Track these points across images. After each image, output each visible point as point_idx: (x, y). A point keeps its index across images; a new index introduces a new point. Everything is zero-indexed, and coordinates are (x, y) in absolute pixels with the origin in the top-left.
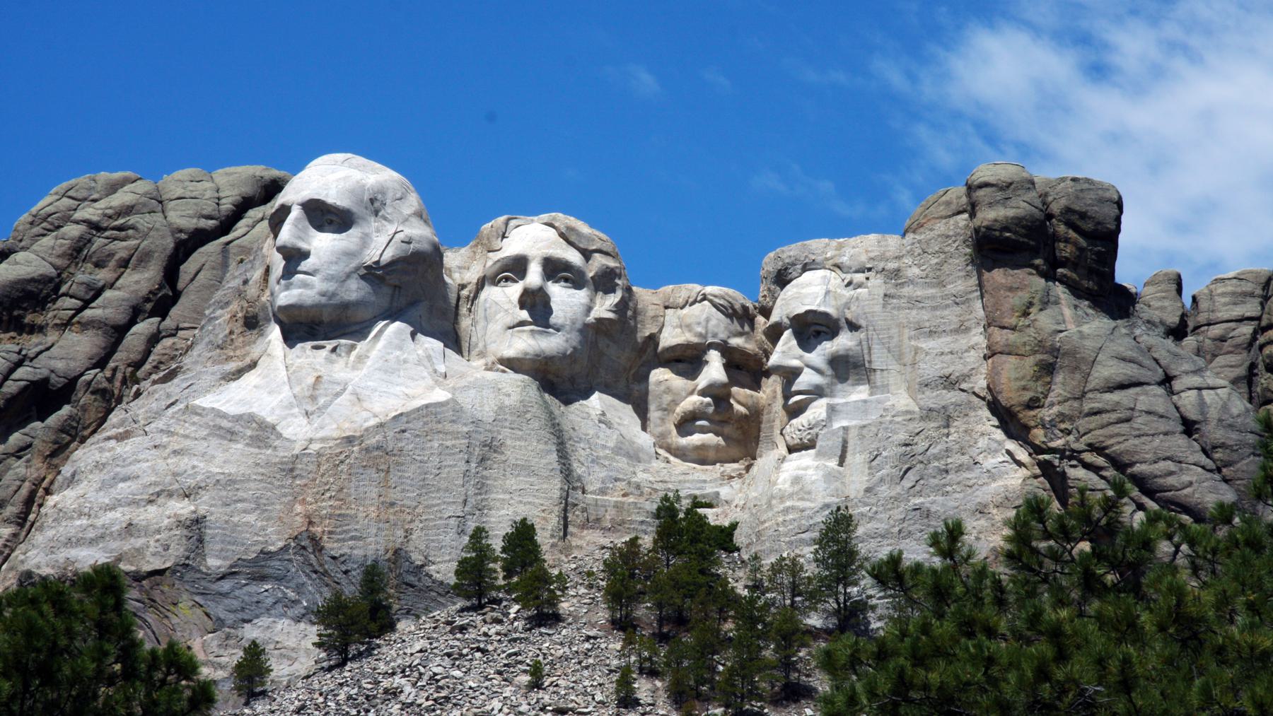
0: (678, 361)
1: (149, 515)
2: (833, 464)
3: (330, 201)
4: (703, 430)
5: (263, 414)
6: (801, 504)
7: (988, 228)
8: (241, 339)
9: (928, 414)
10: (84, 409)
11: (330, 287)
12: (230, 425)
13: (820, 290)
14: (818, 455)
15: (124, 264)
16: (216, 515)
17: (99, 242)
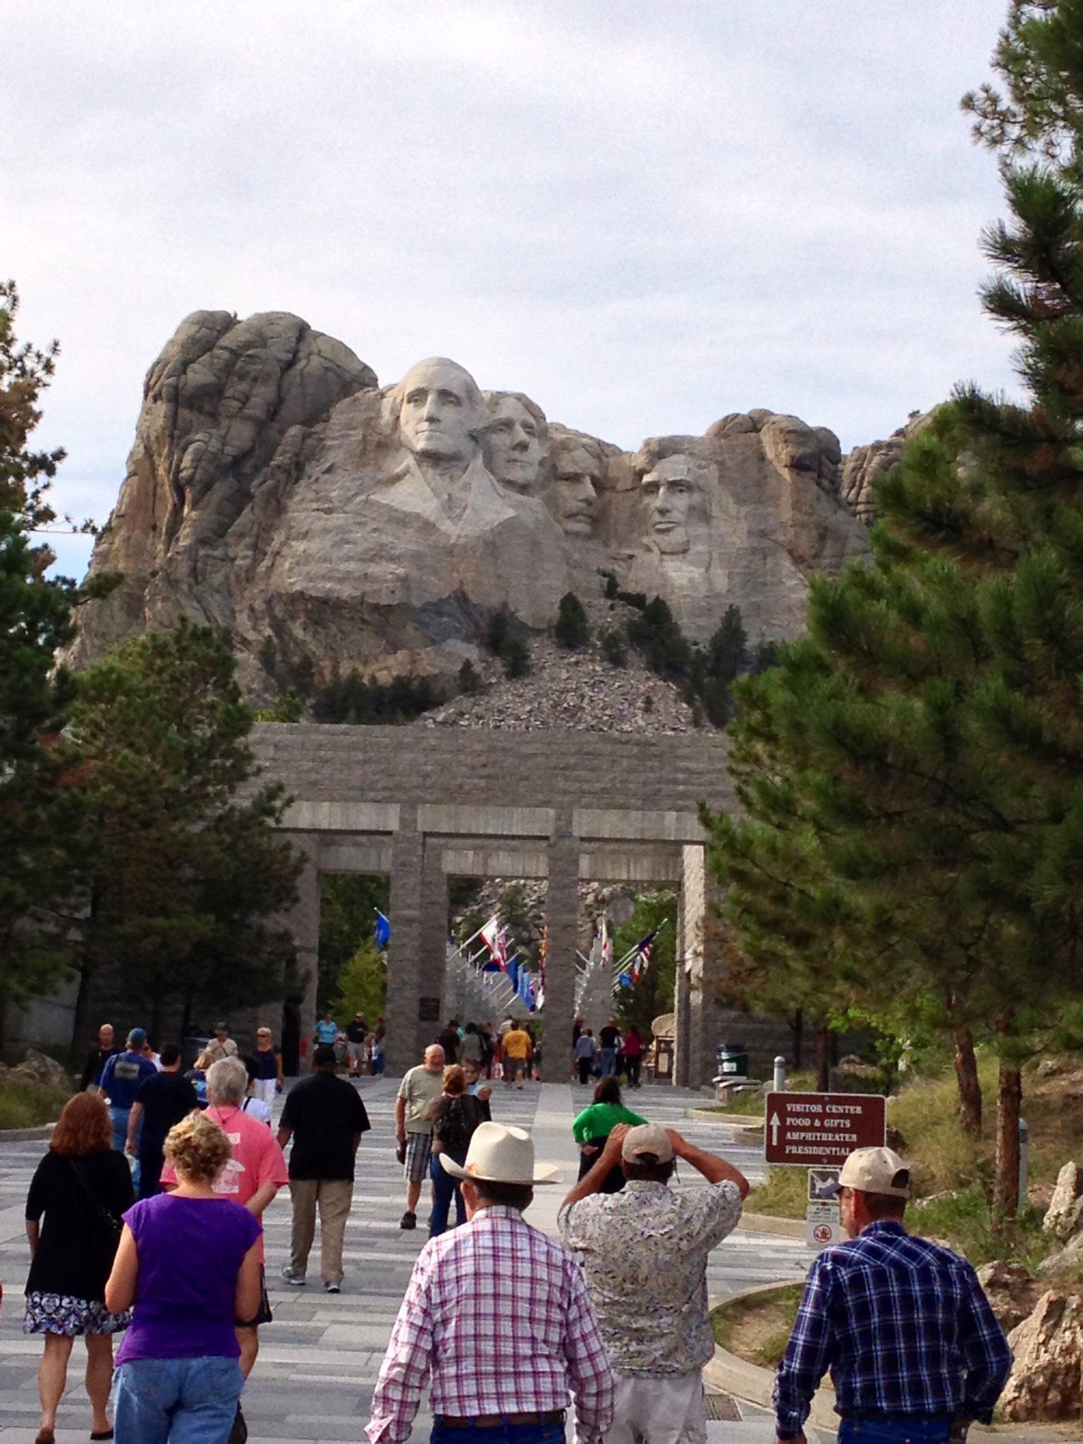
0: (566, 479)
1: (373, 569)
2: (703, 570)
3: (455, 392)
4: (581, 521)
5: (426, 516)
6: (694, 594)
7: (800, 458)
8: (372, 455)
9: (754, 551)
10: (278, 481)
11: (451, 441)
12: (402, 516)
13: (685, 467)
14: (691, 563)
15: (255, 380)
16: (415, 573)
17: (239, 364)
